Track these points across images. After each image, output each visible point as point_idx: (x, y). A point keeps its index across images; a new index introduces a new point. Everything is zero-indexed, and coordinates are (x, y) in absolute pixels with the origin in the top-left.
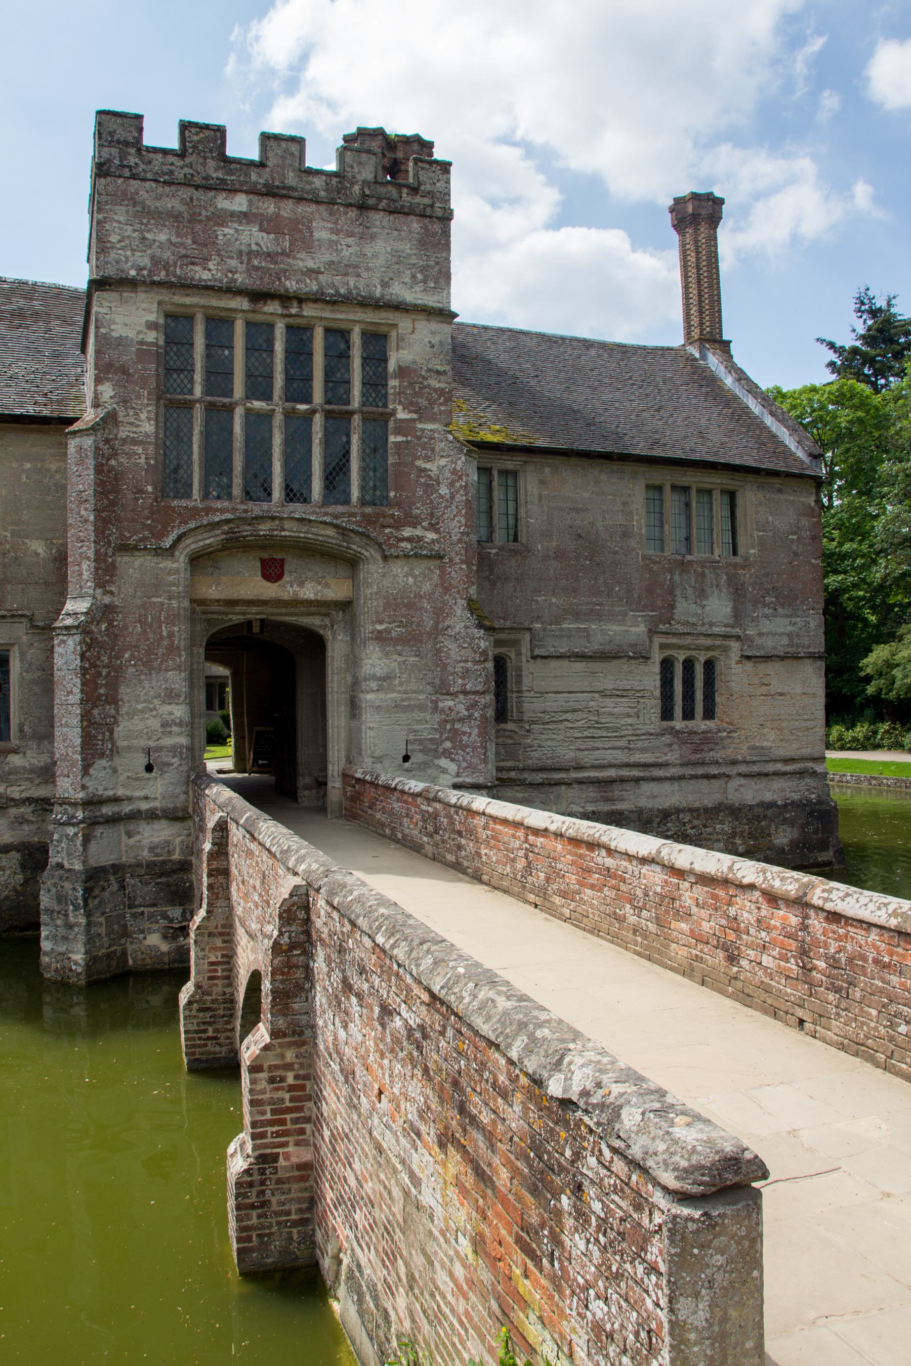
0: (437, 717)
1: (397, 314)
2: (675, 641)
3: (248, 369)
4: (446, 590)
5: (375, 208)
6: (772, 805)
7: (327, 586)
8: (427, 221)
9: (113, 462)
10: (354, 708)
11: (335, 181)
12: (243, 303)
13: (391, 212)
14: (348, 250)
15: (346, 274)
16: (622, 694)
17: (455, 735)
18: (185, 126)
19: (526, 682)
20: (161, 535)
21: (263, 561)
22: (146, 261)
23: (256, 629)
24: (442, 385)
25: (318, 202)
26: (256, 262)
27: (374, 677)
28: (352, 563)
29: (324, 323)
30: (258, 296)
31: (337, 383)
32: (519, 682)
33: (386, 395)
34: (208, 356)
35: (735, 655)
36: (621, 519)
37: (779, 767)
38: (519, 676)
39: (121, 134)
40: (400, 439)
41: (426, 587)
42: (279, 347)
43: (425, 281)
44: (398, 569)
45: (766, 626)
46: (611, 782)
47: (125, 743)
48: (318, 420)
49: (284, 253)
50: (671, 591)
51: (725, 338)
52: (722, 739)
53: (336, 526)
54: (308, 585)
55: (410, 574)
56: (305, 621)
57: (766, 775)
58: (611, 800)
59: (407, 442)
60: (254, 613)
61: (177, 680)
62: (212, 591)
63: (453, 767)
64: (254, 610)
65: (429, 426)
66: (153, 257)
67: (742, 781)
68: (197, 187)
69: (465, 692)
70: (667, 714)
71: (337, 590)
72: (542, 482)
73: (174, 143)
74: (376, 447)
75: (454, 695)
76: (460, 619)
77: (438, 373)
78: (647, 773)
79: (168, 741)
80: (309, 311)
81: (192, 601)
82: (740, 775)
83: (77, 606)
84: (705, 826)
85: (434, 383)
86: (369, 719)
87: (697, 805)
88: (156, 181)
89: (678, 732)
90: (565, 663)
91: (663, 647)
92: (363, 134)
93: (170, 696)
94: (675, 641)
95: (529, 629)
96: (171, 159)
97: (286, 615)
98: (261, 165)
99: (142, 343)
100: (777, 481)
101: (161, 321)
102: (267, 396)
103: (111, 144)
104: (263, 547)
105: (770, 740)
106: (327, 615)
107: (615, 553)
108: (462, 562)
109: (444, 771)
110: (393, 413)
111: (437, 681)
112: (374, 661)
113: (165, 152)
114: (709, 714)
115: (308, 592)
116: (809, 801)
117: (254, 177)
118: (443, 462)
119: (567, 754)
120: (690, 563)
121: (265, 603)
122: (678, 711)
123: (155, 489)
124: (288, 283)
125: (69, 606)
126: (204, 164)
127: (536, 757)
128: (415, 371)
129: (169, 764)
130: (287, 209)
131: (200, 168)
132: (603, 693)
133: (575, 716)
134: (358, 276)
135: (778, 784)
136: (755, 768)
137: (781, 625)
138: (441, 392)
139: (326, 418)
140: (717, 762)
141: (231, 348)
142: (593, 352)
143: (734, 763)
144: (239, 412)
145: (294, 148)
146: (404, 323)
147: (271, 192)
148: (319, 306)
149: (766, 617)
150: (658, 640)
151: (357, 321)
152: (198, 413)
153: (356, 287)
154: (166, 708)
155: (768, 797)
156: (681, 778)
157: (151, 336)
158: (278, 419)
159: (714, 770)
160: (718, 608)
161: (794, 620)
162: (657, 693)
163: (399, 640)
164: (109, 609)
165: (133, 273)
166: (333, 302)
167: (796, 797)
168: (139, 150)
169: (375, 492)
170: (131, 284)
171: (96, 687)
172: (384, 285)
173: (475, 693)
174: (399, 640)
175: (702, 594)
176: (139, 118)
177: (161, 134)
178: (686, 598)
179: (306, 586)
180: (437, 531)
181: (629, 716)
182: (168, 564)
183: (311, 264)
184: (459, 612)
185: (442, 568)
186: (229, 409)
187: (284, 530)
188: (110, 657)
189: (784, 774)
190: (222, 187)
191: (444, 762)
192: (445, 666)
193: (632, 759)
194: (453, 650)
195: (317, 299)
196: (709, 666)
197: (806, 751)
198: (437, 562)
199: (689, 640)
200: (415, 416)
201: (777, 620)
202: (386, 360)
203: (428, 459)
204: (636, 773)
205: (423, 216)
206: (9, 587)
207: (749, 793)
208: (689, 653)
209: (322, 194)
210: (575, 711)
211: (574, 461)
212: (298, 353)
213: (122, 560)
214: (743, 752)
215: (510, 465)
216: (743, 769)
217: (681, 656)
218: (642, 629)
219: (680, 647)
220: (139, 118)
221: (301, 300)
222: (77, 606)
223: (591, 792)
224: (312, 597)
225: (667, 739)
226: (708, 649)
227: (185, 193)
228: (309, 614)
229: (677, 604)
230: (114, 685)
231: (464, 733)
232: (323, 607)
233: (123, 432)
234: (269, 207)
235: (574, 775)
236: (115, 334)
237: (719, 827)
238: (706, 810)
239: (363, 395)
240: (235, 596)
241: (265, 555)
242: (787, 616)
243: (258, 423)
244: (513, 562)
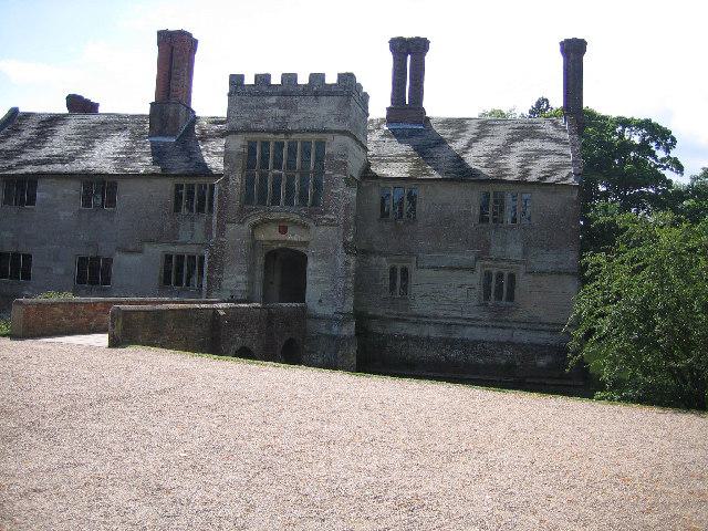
5: (322, 95)
18: (256, 76)
44: (322, 230)
46: (450, 325)
60: (284, 245)
62: (262, 236)
74: (317, 185)
78: (471, 322)
80: (294, 137)
91: (483, 266)
93: (240, 273)
102: (280, 168)
114: (511, 298)
135: (547, 335)
146: (329, 137)
147: (284, 94)
150: (479, 264)
166: (319, 132)
169: (315, 203)
177: (249, 80)
179: (294, 236)
195: (300, 131)
196: (512, 277)
204: (465, 322)
207: (525, 337)
212: (292, 151)
213: (228, 226)
216: (525, 326)
217: (495, 271)
218: (472, 257)
243: (277, 179)
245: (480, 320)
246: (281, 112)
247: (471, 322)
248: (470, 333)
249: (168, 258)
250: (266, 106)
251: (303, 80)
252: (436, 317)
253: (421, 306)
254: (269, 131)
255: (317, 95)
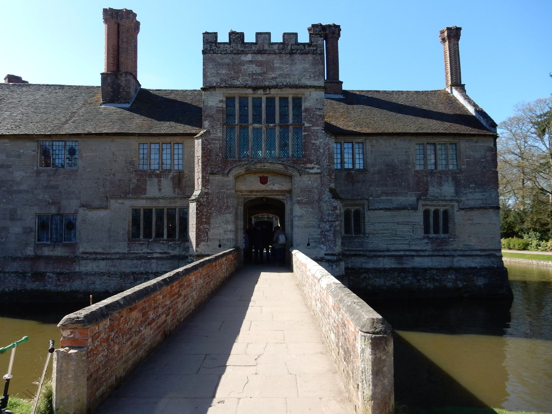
0: (320, 230)
1: (304, 90)
2: (429, 203)
3: (280, 113)
4: (323, 185)
5: (296, 53)
6: (475, 268)
7: (283, 185)
8: (315, 55)
9: (209, 146)
10: (292, 227)
11: (281, 46)
12: (250, 91)
13: (301, 54)
14: (286, 68)
15: (286, 78)
16: (407, 223)
17: (325, 236)
19: (367, 219)
20: (223, 170)
21: (260, 177)
22: (219, 80)
23: (265, 200)
24: (321, 113)
25: (275, 53)
26: (255, 77)
27: (297, 216)
28: (291, 177)
29: (279, 95)
30: (255, 89)
31: (284, 116)
32: (364, 219)
33: (301, 119)
34: (240, 110)
35: (456, 209)
36: (405, 158)
37: (478, 253)
38: (364, 217)
39: (210, 39)
40: (306, 133)
41: (315, 185)
42: (264, 105)
43: (314, 77)
45: (470, 196)
46: (401, 256)
47: (212, 238)
48: (277, 129)
49: (264, 73)
50: (427, 184)
51: (462, 83)
52: (451, 241)
53: (283, 164)
54: (276, 185)
55: (310, 180)
56: (277, 197)
57: (472, 256)
58: (402, 264)
59: (308, 134)
60: (259, 195)
61: (230, 217)
63: (325, 248)
64: (259, 194)
65: (316, 128)
66: (221, 79)
67: (461, 258)
68: (235, 54)
69: (328, 221)
70: (427, 231)
71: (286, 186)
72: (372, 146)
73: (227, 40)
75: (325, 222)
76: (327, 196)
77: (319, 109)
78: (418, 253)
79: (226, 237)
80: (273, 91)
81: (236, 191)
82: (459, 256)
83: (197, 193)
84: (443, 276)
85: (318, 113)
86: (296, 230)
87: (440, 267)
88: (221, 53)
89: (430, 238)
90: (382, 212)
91: (423, 205)
92: (314, 26)
93: (227, 222)
94: (429, 203)
95: (368, 200)
96: (226, 45)
97: (272, 195)
98: (256, 44)
99: (218, 107)
100: (475, 139)
101: (224, 99)
102: (260, 122)
103: (207, 43)
104: (259, 173)
105: (474, 243)
106: (285, 195)
107: (403, 170)
108: (327, 175)
109: (322, 249)
110: (304, 124)
111: (320, 217)
112: (298, 210)
113: (224, 43)
114: (446, 231)
115: (276, 187)
116: (494, 268)
117: (253, 48)
118: (321, 140)
119: (383, 246)
120: (436, 173)
121: (262, 191)
122: (432, 230)
123: (222, 154)
124: (266, 83)
125: (194, 193)
126: (237, 46)
127: (370, 247)
128: (311, 109)
129: (226, 245)
130: (265, 56)
131: (235, 47)
132: (398, 223)
133: (387, 232)
134: (290, 78)
135: (478, 260)
136: (467, 253)
137: (478, 196)
138: (321, 116)
139: (280, 128)
140: (448, 250)
141: (248, 107)
142: (404, 96)
143: (456, 250)
144: (250, 128)
145: (267, 36)
146: (307, 92)
147: (260, 52)
148: (276, 90)
149: (470, 193)
151: (290, 93)
152: (237, 129)
153: (289, 82)
154: (225, 226)
155: (473, 265)
156: (433, 256)
157: (220, 105)
158: (264, 129)
159: (446, 253)
160: (448, 189)
161: (484, 193)
162: (422, 223)
163: (305, 203)
164: (206, 193)
165: (215, 84)
167: (486, 265)
168: (216, 44)
170: (214, 88)
171: (202, 219)
172: (299, 80)
173: (332, 221)
174: (305, 203)
175: (440, 184)
176: (216, 33)
177: (223, 38)
178: (433, 187)
179: (276, 186)
180: (319, 165)
181: (409, 232)
182: (226, 179)
183: (273, 76)
184: (326, 193)
185: (321, 177)
186: (247, 127)
187: (265, 166)
188: (207, 210)
189: (481, 256)
190: (243, 52)
191: (322, 246)
192: (322, 212)
193: (411, 248)
194: (324, 206)
195: (275, 87)
197: (493, 247)
198: (319, 176)
199: (434, 203)
200: (311, 125)
201: (476, 194)
202: (301, 106)
203: (316, 140)
205: (313, 54)
206: (187, 188)
208: (435, 208)
209: (277, 51)
210: (387, 230)
211: (385, 137)
213: (211, 177)
214: (461, 246)
215: (360, 140)
216: (460, 253)
217: (432, 209)
218: (414, 198)
219: (431, 205)
220: (216, 33)
221: (270, 88)
222: (197, 193)
223: (393, 261)
224: (277, 189)
225: (426, 241)
226: (444, 206)
227: (231, 56)
228: (278, 195)
229: (429, 189)
230: (208, 218)
231: (328, 236)
232: (283, 192)
233: (212, 136)
234: (259, 58)
235: (386, 253)
236: (209, 105)
237: (449, 276)
238: (444, 269)
239: (293, 119)
240: (251, 189)
241: (261, 175)
242: (481, 192)
244: (361, 176)
245: (426, 250)
246: (258, 70)
247: (418, 253)
248: (419, 262)
249: (136, 212)
250: (242, 63)
251: (277, 38)
252: (388, 250)
253: (376, 242)
254: (246, 87)
255: (291, 53)
